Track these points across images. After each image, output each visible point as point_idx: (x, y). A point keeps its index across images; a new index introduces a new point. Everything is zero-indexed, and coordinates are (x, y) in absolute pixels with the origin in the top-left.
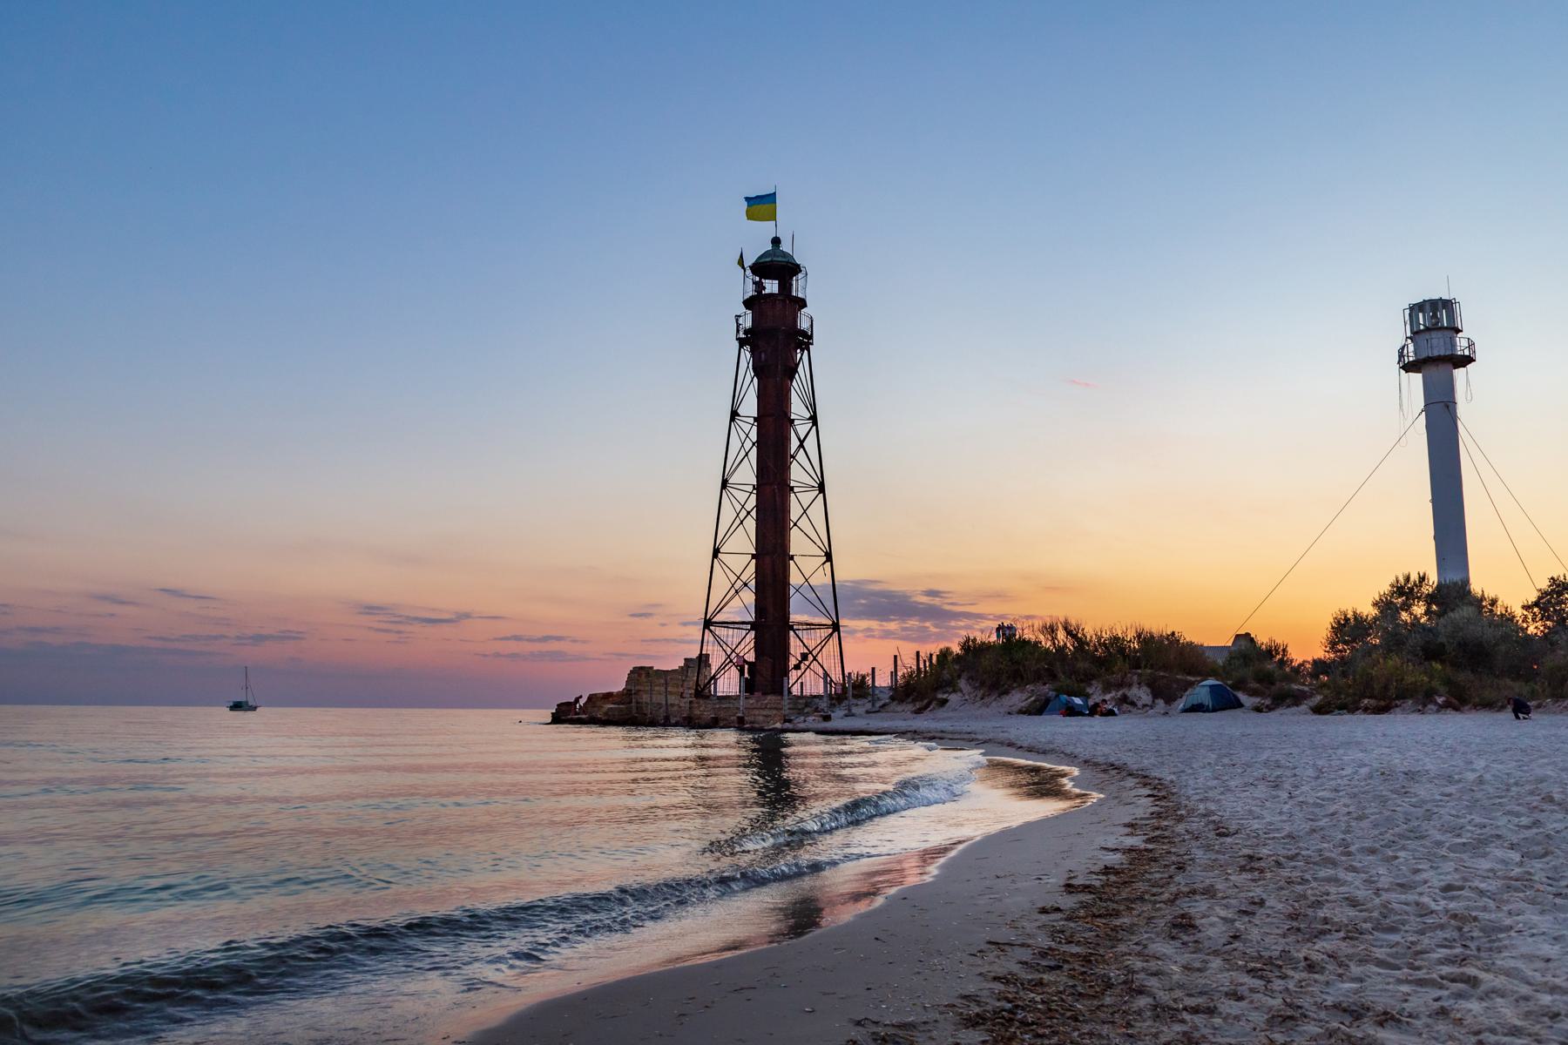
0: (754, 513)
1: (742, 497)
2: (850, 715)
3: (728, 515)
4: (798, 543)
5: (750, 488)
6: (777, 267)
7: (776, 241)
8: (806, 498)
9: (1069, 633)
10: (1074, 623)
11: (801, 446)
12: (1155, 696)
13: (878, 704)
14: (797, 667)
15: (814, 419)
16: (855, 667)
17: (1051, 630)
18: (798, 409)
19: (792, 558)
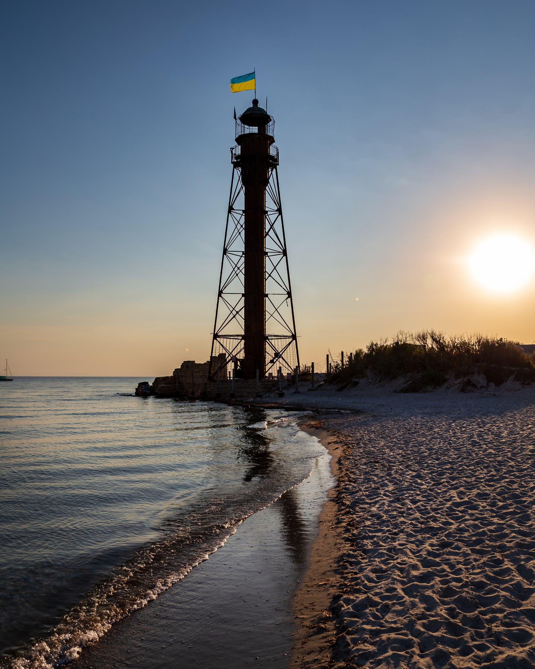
0: (243, 271)
1: (235, 259)
2: (297, 392)
3: (228, 269)
4: (271, 287)
5: (241, 254)
6: (256, 116)
7: (255, 102)
8: (275, 259)
9: (434, 340)
11: (272, 226)
12: (490, 379)
13: (316, 385)
14: (272, 361)
15: (279, 210)
16: (305, 363)
17: (423, 338)
18: (270, 205)
19: (267, 296)
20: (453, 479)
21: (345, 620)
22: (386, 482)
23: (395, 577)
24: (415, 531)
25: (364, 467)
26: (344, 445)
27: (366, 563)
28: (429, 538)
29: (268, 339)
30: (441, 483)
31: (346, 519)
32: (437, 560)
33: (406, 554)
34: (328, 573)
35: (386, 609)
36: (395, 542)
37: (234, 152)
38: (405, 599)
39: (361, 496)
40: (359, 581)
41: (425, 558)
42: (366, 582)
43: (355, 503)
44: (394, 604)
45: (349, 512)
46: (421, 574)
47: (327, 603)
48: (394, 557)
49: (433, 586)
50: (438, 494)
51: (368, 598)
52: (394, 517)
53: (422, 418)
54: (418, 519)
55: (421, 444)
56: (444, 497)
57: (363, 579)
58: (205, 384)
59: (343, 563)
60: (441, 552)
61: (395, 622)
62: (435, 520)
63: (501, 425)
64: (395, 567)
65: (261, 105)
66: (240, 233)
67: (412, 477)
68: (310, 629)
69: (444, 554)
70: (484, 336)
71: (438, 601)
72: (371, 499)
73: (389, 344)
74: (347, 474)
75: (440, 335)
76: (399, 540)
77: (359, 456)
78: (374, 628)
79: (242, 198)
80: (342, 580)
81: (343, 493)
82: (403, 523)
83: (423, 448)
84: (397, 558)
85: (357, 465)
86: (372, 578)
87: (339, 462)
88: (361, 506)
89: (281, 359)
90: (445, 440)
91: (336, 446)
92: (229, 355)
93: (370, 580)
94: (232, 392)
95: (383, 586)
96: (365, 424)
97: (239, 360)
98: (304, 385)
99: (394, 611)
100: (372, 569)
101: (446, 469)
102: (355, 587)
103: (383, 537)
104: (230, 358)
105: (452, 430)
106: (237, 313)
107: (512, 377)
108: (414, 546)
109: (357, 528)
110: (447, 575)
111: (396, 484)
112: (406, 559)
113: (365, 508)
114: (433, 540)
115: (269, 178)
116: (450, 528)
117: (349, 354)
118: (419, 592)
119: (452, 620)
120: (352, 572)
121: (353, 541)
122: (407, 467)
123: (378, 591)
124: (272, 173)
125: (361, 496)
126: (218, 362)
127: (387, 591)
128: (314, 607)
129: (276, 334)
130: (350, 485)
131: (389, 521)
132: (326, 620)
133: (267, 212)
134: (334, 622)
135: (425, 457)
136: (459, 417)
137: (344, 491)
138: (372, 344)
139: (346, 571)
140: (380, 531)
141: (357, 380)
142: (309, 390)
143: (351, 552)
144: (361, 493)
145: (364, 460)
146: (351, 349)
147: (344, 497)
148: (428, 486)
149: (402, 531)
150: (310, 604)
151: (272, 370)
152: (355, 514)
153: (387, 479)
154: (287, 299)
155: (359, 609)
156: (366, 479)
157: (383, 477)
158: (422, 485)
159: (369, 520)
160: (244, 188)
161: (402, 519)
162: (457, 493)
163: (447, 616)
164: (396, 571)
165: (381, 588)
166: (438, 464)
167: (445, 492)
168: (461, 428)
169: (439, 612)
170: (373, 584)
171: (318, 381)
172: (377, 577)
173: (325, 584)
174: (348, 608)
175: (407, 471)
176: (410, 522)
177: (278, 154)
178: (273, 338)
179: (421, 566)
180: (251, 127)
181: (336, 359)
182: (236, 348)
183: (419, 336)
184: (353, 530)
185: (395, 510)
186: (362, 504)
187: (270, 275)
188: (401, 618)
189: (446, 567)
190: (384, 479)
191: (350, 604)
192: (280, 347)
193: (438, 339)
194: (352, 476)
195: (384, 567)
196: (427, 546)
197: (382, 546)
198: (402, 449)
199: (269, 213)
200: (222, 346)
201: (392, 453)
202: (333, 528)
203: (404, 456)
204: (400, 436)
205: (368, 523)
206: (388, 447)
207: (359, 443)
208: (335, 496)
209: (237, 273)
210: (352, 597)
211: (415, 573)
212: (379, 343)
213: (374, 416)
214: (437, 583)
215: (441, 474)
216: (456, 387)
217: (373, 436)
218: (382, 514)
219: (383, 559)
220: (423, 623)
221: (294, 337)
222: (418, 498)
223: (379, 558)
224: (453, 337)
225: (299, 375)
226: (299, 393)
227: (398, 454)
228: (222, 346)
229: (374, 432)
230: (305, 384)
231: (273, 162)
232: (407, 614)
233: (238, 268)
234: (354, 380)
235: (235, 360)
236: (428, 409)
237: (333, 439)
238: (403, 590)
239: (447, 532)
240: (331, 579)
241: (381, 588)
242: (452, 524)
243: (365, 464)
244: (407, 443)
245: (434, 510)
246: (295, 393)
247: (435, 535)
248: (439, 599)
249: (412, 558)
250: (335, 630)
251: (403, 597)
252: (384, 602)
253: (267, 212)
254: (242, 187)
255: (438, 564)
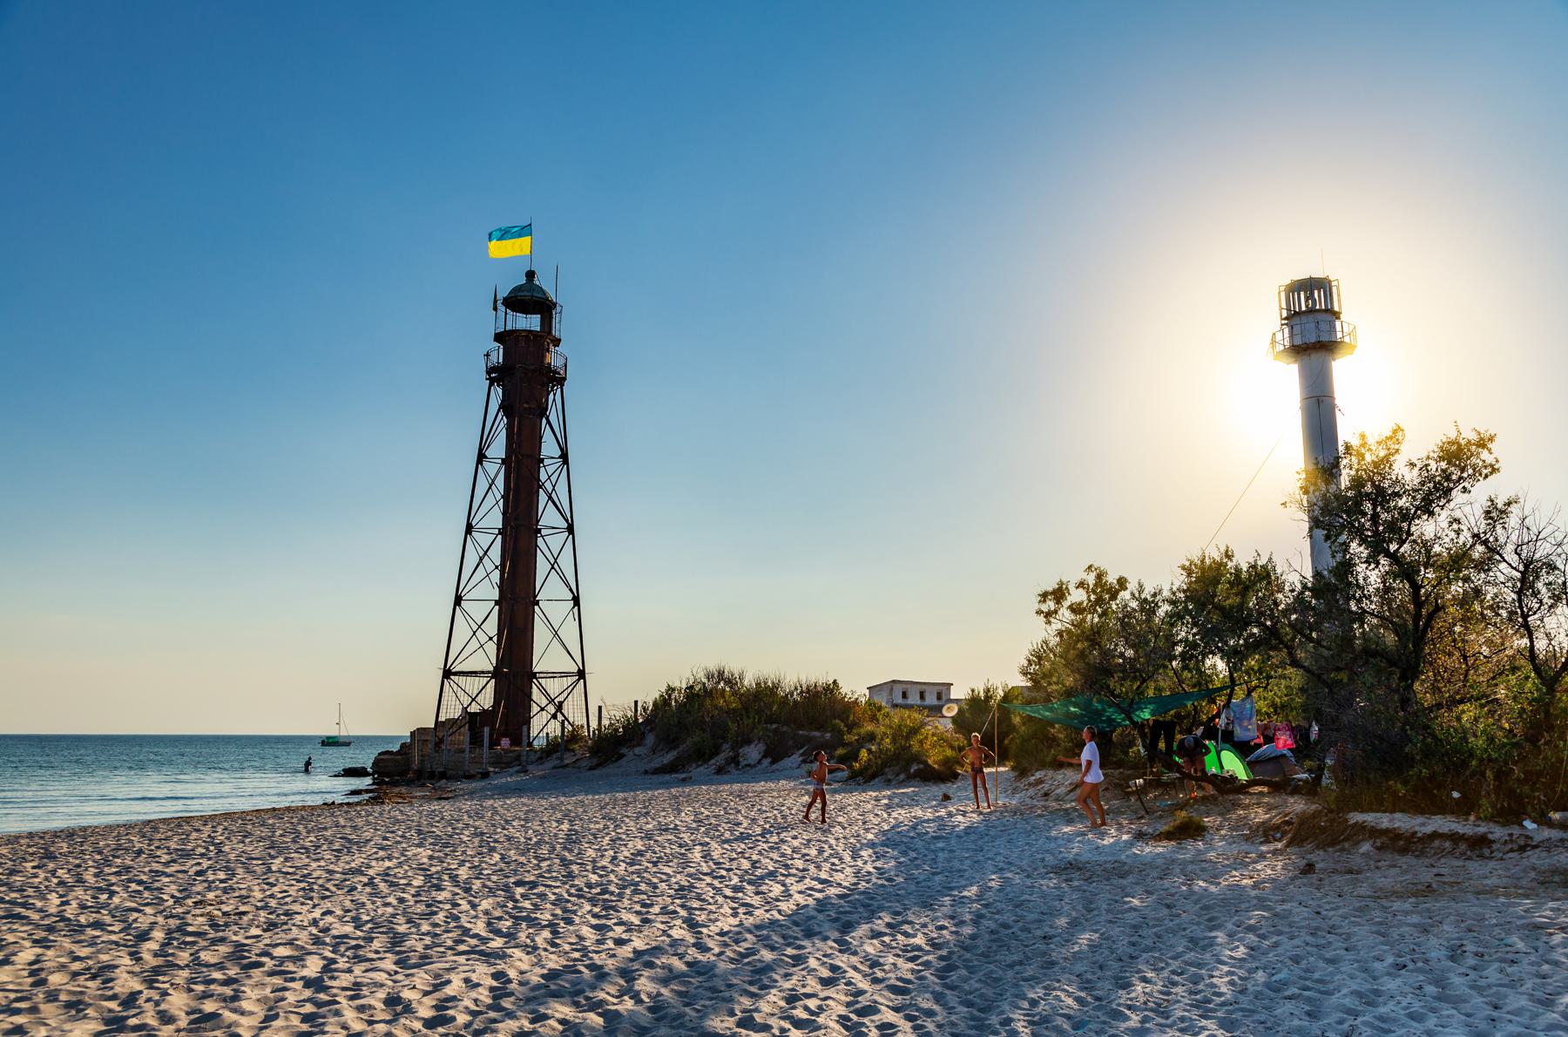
7: (530, 275)
18: (549, 448)
19: (537, 603)
65: (544, 282)
199: (546, 462)
221: (581, 674)
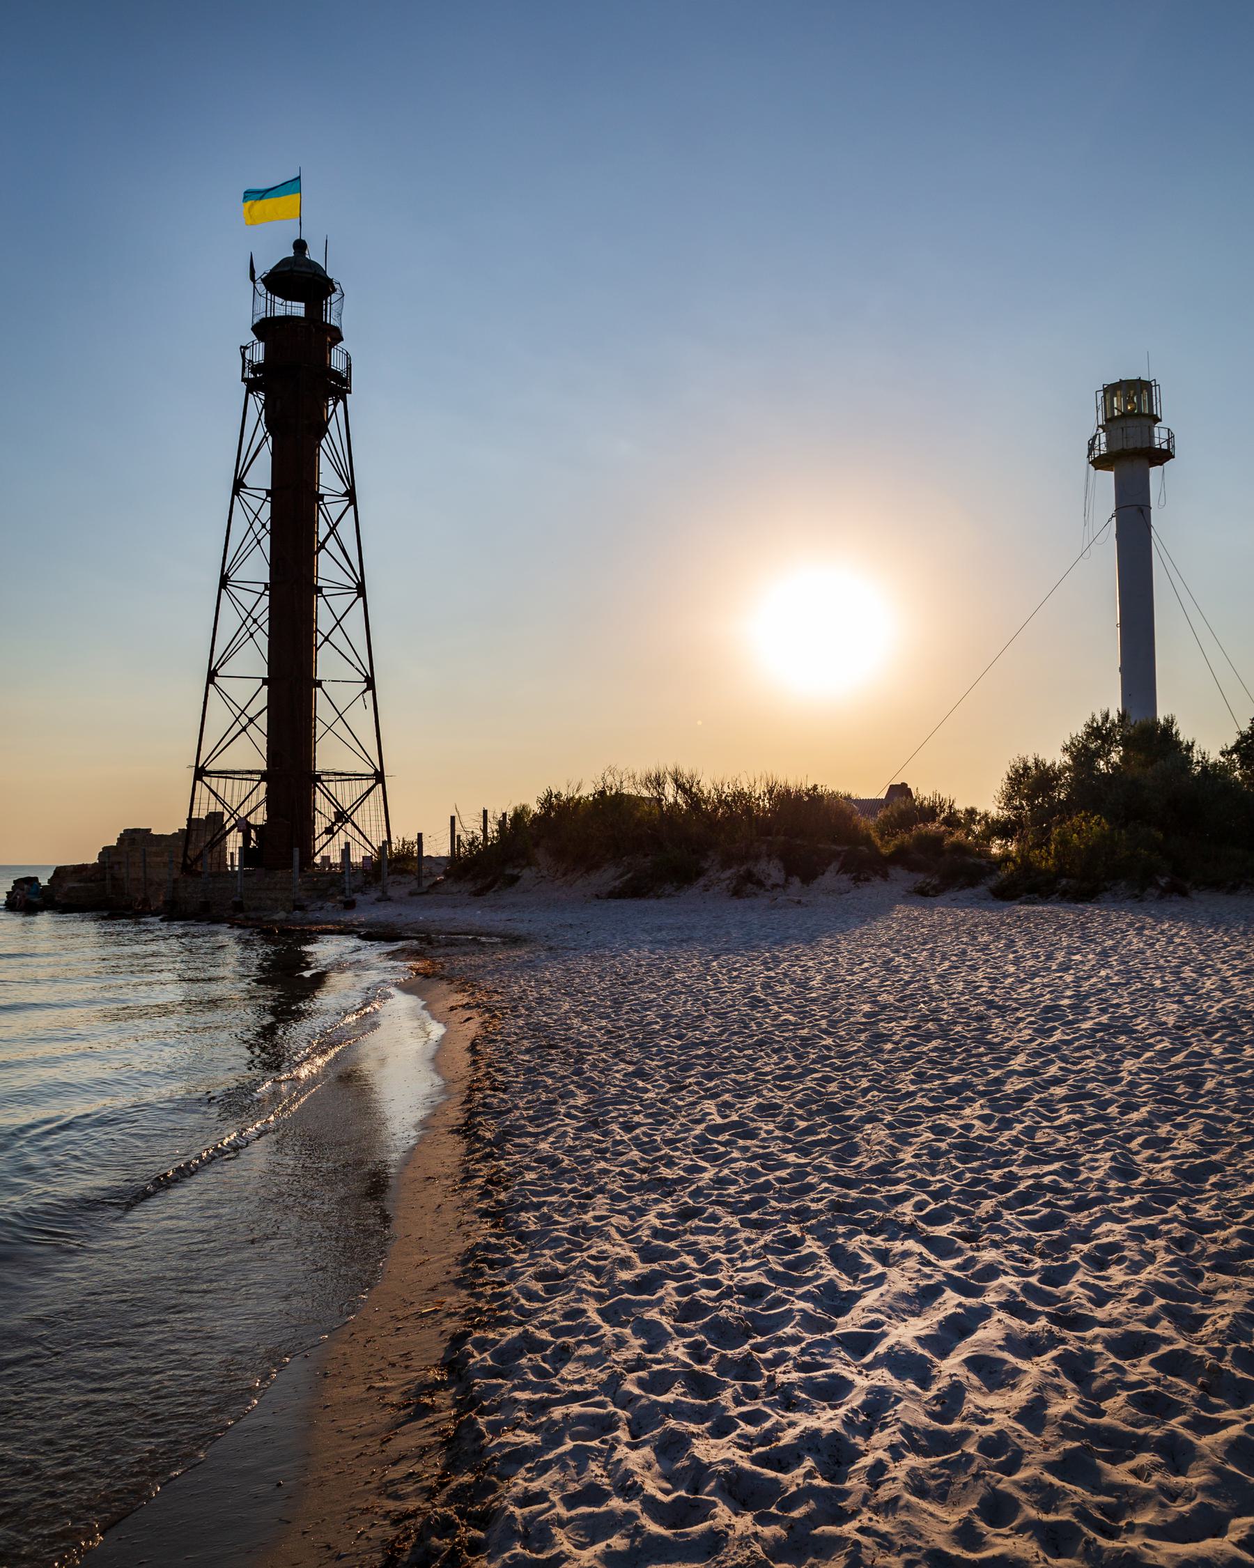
0: (266, 627)
2: (385, 899)
3: (230, 621)
4: (327, 664)
5: (261, 588)
6: (300, 278)
7: (300, 246)
9: (679, 786)
10: (686, 773)
11: (332, 530)
12: (789, 872)
13: (426, 883)
14: (329, 831)
15: (351, 495)
16: (403, 833)
17: (658, 782)
18: (329, 480)
19: (319, 684)
20: (710, 1077)
21: (474, 1385)
22: (572, 1087)
23: (583, 1286)
24: (629, 1189)
25: (527, 1058)
26: (484, 1013)
27: (523, 1260)
28: (656, 1201)
29: (322, 782)
30: (685, 1087)
31: (485, 1169)
32: (672, 1245)
33: (608, 1238)
34: (441, 1288)
35: (563, 1355)
36: (586, 1213)
37: (248, 356)
38: (602, 1332)
39: (517, 1120)
40: (508, 1299)
41: (648, 1243)
42: (523, 1301)
43: (505, 1135)
44: (579, 1344)
45: (490, 1156)
46: (637, 1276)
47: (438, 1351)
48: (582, 1244)
49: (661, 1300)
50: (678, 1109)
51: (526, 1336)
52: (586, 1161)
53: (652, 952)
54: (635, 1162)
55: (647, 1005)
56: (689, 1115)
57: (516, 1295)
58: (175, 881)
59: (475, 1263)
60: (681, 1228)
61: (581, 1381)
62: (670, 1163)
63: (810, 964)
64: (583, 1265)
66: (259, 542)
67: (625, 1075)
68: (399, 1410)
69: (685, 1232)
70: (781, 781)
71: (670, 1329)
72: (538, 1126)
73: (585, 795)
74: (489, 1073)
75: (692, 777)
76: (594, 1209)
77: (516, 1034)
78: (537, 1396)
79: (265, 460)
80: (473, 1300)
81: (479, 1114)
82: (605, 1172)
83: (651, 1015)
84: (590, 1247)
85: (511, 1053)
86: (536, 1292)
87: (473, 1049)
88: (518, 1141)
89: (349, 825)
90: (696, 995)
91: (468, 1014)
92: (232, 816)
93: (531, 1296)
94: (237, 899)
95: (557, 1306)
96: (531, 965)
97: (255, 827)
98: (400, 883)
99: (580, 1358)
100: (535, 1273)
101: (697, 1057)
102: (499, 1314)
103: (560, 1205)
104: (233, 822)
105: (712, 976)
106: (251, 720)
107: (834, 866)
108: (625, 1220)
109: (506, 1189)
110: (690, 1276)
111: (592, 1091)
112: (607, 1247)
113: (525, 1145)
114: (665, 1206)
115: (329, 420)
116: (700, 1179)
117: (499, 816)
118: (633, 1315)
119: (697, 1367)
120: (494, 1282)
121: (497, 1215)
122: (616, 1055)
123: (546, 1318)
124: (334, 410)
125: (517, 1120)
126: (206, 831)
127: (566, 1316)
128: (408, 1363)
129: (338, 770)
130: (494, 1096)
131: (575, 1170)
132: (437, 1386)
133: (321, 497)
134: (453, 1390)
135: (656, 1032)
136: (727, 949)
137: (481, 1109)
138: (550, 794)
139: (481, 1281)
140: (556, 1191)
141: (516, 872)
142: (411, 894)
143: (493, 1240)
144: (517, 1113)
145: (525, 1042)
146: (503, 805)
147: (480, 1124)
148: (658, 1094)
149: (601, 1190)
150: (401, 1356)
151: (329, 850)
152: (502, 1158)
153: (573, 1082)
154: (364, 692)
155: (506, 1359)
156: (529, 1083)
157: (564, 1077)
158: (646, 1091)
159: (533, 1169)
160: (270, 439)
161: (603, 1165)
162: (717, 1105)
163: (688, 1360)
164: (586, 1274)
165: (554, 1311)
166: (680, 1048)
167: (694, 1104)
168: (729, 971)
169: (673, 1353)
170: (537, 1305)
171: (432, 875)
172: (548, 1290)
173: (436, 1311)
174: (483, 1360)
175: (616, 1064)
176: (618, 1170)
177: (349, 368)
178: (332, 778)
179: (638, 1260)
180: (289, 303)
181: (470, 827)
182: (248, 800)
183: (648, 779)
184: (499, 1193)
185: (588, 1147)
186: (519, 1136)
187: (326, 639)
188: (593, 1371)
189: (688, 1260)
190: (567, 1081)
191: (486, 1350)
192: (348, 798)
193: (687, 786)
194: (500, 1078)
195: (561, 1267)
196: (652, 1219)
197: (558, 1223)
198: (608, 1017)
199: (326, 499)
200: (216, 795)
201: (585, 1027)
202: (455, 1190)
203: (610, 1032)
204: (604, 989)
205: (531, 1176)
206: (578, 1014)
207: (515, 1007)
208: (462, 1121)
209: (252, 630)
210: (491, 1336)
211: (625, 1275)
212: (564, 792)
213: (551, 948)
214: (669, 1294)
215: (686, 1067)
216: (724, 885)
217: (546, 990)
218: (561, 1156)
219: (560, 1250)
220: (639, 1378)
221: (379, 777)
222: (636, 1119)
223: (551, 1249)
224: (718, 782)
225: (390, 861)
226: (389, 899)
227: (599, 1029)
228: (216, 795)
229: (548, 982)
230: (403, 880)
231: (339, 386)
232: (606, 1360)
233: (255, 621)
234: (509, 871)
235: (244, 826)
236: (664, 933)
237: (462, 999)
238: (600, 1312)
239: (694, 1187)
240: (449, 1300)
241: (554, 1311)
242: (704, 1169)
243: (528, 1051)
244: (617, 1004)
245: (669, 1142)
246: (379, 900)
247: (670, 1194)
248: (672, 1326)
249: (621, 1245)
250: (453, 1407)
251: (600, 1327)
252: (559, 1341)
253: (321, 497)
254: (265, 437)
255: (674, 1254)
